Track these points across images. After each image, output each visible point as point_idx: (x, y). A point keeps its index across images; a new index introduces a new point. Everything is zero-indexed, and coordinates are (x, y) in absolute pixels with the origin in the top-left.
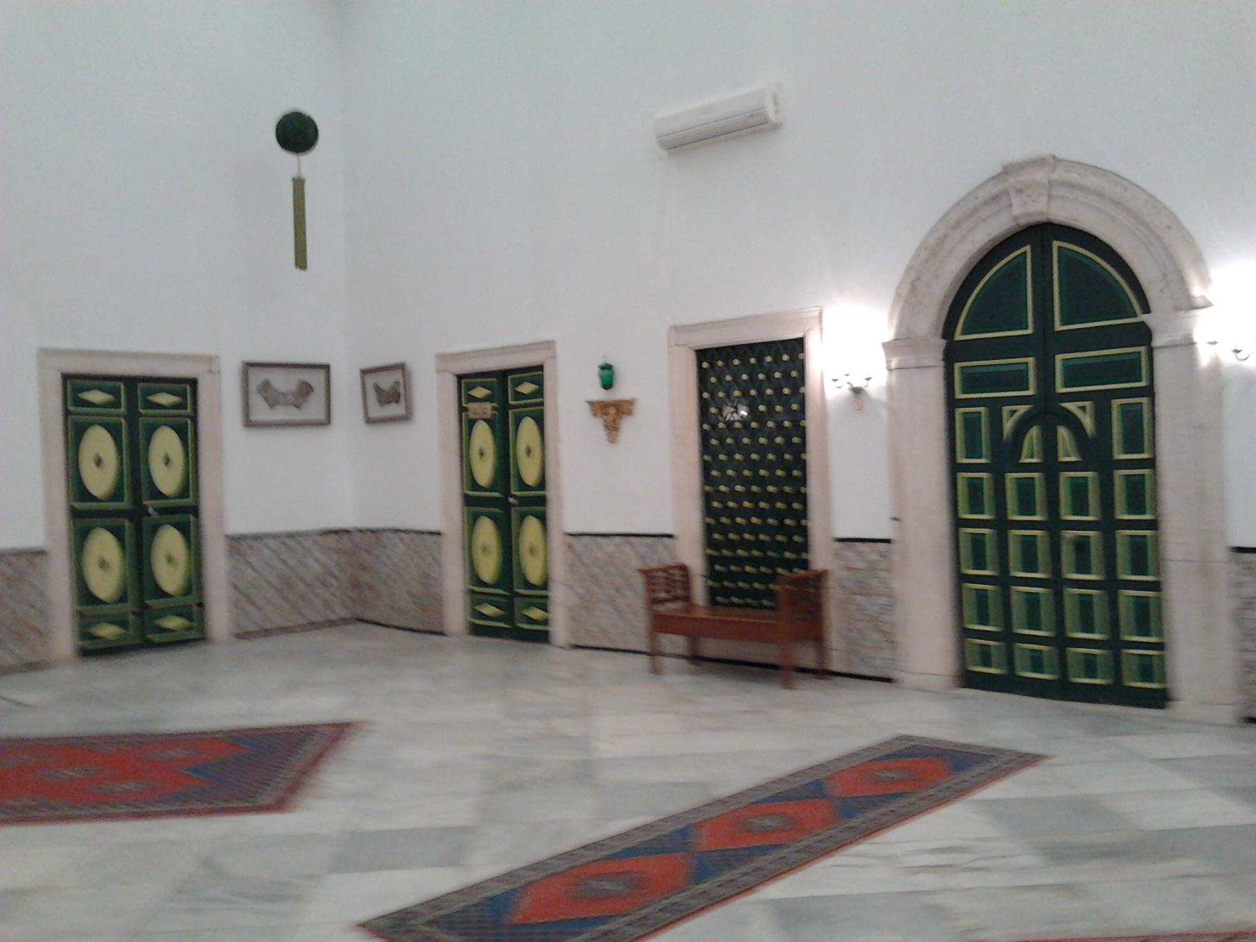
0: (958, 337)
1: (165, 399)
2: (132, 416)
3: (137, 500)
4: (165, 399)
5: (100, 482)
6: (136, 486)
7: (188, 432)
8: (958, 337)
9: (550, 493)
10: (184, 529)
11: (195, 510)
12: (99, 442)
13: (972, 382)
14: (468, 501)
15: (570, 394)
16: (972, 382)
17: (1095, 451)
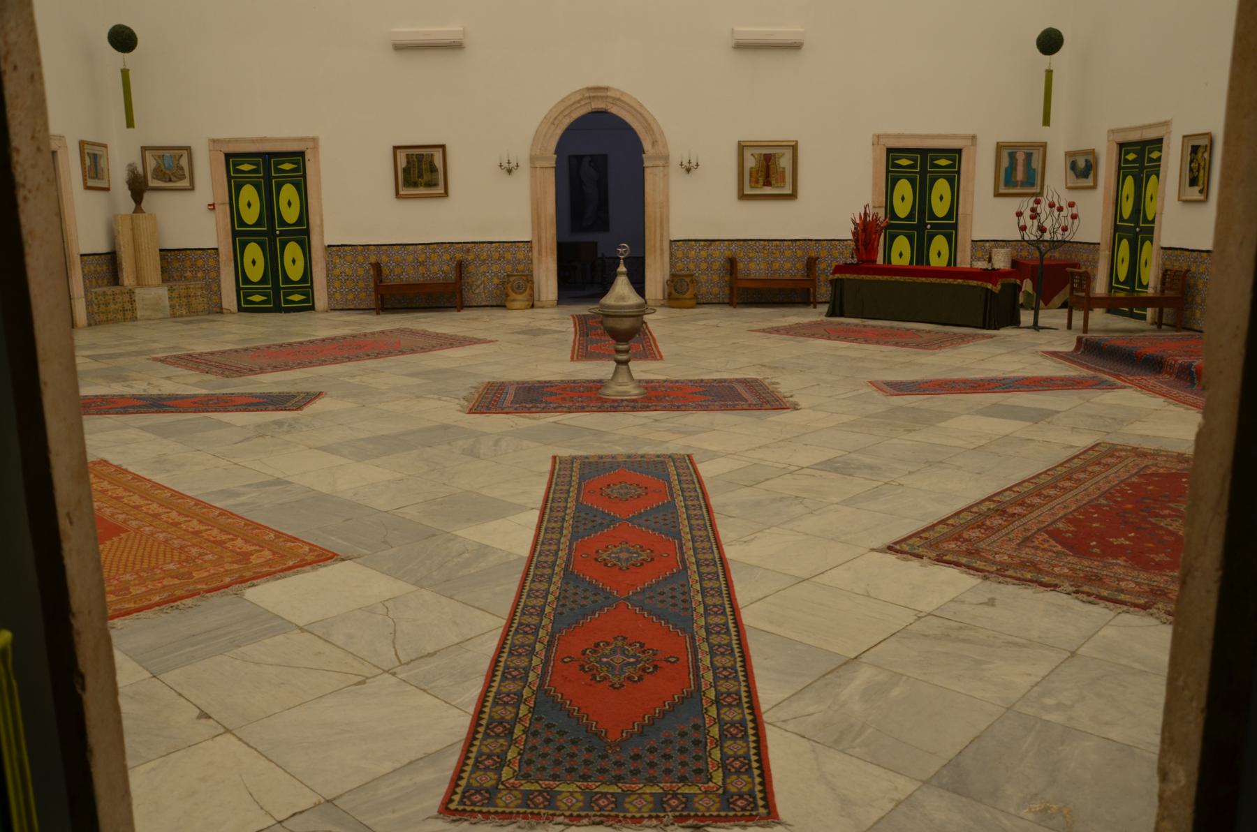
1: (943, 162)
2: (923, 173)
3: (921, 218)
4: (943, 162)
5: (902, 209)
6: (922, 212)
9: (1156, 225)
10: (949, 238)
11: (955, 227)
14: (1116, 228)
15: (1173, 161)
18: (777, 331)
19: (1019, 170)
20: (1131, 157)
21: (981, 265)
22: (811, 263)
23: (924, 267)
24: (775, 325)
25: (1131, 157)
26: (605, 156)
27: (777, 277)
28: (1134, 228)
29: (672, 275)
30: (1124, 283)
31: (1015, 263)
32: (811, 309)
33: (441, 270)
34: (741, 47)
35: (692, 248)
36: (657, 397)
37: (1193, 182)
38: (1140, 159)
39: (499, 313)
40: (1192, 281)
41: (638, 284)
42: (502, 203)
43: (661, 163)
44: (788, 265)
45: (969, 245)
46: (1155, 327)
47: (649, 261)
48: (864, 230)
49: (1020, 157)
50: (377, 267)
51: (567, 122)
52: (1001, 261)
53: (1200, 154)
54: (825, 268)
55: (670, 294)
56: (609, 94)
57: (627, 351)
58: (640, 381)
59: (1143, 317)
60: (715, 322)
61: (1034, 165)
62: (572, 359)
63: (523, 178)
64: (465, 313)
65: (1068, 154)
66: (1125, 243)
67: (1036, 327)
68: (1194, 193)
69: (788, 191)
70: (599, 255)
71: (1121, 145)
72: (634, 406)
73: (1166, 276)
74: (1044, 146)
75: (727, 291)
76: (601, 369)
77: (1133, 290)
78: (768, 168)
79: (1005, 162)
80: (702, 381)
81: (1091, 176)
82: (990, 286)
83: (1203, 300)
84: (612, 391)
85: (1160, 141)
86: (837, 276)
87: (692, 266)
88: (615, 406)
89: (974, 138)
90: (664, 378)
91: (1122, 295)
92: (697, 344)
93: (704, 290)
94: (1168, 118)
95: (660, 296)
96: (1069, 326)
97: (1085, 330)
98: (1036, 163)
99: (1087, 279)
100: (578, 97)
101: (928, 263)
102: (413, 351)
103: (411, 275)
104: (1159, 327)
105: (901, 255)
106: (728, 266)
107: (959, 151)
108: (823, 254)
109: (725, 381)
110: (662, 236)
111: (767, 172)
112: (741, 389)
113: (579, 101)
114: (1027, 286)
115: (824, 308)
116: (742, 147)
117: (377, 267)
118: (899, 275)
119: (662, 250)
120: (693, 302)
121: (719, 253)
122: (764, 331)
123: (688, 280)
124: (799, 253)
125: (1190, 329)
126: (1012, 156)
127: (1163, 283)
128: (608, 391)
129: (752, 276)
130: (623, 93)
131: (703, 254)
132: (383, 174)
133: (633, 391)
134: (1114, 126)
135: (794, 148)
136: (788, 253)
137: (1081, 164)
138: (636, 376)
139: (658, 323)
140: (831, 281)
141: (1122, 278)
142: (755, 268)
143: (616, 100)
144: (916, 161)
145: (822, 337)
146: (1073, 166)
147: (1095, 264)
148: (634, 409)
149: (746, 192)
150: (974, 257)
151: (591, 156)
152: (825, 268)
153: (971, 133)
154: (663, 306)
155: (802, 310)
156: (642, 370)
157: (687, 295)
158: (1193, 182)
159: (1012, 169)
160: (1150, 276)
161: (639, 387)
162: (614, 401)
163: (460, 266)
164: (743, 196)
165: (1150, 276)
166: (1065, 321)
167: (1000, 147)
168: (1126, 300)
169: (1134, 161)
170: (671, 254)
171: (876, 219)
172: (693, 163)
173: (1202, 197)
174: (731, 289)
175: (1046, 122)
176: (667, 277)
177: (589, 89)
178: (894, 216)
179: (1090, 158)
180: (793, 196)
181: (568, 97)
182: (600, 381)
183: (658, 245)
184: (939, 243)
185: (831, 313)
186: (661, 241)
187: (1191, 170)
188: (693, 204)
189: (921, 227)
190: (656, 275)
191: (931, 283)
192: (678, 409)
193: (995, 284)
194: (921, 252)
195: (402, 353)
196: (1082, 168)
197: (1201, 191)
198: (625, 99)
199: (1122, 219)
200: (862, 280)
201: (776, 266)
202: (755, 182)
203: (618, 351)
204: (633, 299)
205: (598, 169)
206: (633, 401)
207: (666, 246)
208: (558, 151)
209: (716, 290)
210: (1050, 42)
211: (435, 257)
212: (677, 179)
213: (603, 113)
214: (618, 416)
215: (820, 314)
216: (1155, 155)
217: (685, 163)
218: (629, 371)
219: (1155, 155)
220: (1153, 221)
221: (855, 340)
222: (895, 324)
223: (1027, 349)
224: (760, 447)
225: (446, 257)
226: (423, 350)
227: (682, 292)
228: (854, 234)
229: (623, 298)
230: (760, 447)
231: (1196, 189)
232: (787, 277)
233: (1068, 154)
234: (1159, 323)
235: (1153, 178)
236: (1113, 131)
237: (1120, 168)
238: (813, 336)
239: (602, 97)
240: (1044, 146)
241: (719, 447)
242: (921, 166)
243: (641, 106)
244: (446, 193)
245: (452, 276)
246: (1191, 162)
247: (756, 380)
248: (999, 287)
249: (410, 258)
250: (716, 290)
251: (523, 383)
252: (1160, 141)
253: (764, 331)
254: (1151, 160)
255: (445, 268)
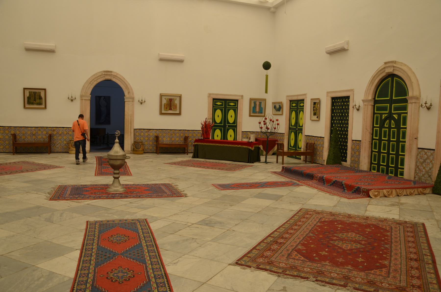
0: (376, 99)
1: (232, 104)
2: (225, 107)
4: (232, 104)
5: (218, 120)
7: (236, 111)
8: (376, 99)
9: (303, 128)
11: (236, 126)
12: (218, 112)
13: (379, 109)
14: (290, 128)
15: (308, 107)
16: (379, 109)
17: (397, 122)
18: (175, 163)
19: (257, 108)
20: (294, 105)
21: (245, 140)
22: (186, 138)
23: (226, 141)
24: (174, 161)
25: (294, 105)
26: (109, 98)
27: (173, 143)
28: (296, 129)
29: (135, 142)
30: (293, 147)
31: (256, 140)
32: (186, 155)
33: (42, 137)
34: (162, 60)
35: (142, 132)
36: (132, 192)
37: (315, 114)
38: (297, 106)
39: (66, 155)
40: (316, 147)
41: (122, 145)
42: (67, 112)
43: (131, 100)
44: (177, 139)
45: (241, 132)
46: (304, 162)
47: (126, 136)
48: (205, 127)
49: (258, 103)
50: (14, 136)
51: (95, 83)
52: (252, 140)
53: (316, 105)
54: (191, 140)
55: (134, 149)
56: (112, 74)
57: (118, 174)
58: (123, 185)
59: (300, 159)
60: (151, 160)
61: (262, 107)
62: (95, 175)
63: (78, 103)
64: (52, 155)
65: (273, 103)
66: (293, 133)
67: (266, 162)
68: (315, 118)
69: (178, 112)
70: (106, 133)
71: (291, 101)
72: (121, 196)
73: (308, 145)
74: (265, 100)
75: (155, 148)
76: (107, 180)
77: (296, 150)
78: (171, 103)
79: (253, 105)
80: (148, 184)
81: (281, 111)
82: (250, 148)
83: (320, 153)
84: (112, 190)
85: (303, 100)
86: (196, 143)
87: (142, 139)
88: (114, 196)
89: (242, 96)
90: (132, 183)
91: (292, 151)
92: (146, 169)
93: (146, 147)
94: (305, 93)
95: (130, 149)
96: (277, 162)
97: (283, 164)
98: (263, 106)
99: (282, 145)
100: (100, 74)
101: (227, 139)
102: (27, 171)
103: (29, 139)
104: (306, 162)
105: (218, 136)
106: (155, 139)
107: (237, 101)
108: (190, 135)
109: (157, 184)
110: (131, 127)
111: (170, 105)
112: (163, 188)
113: (100, 76)
114: (261, 147)
115: (191, 155)
116: (161, 96)
117: (14, 136)
118: (219, 143)
119: (131, 132)
120: (142, 152)
121: (152, 134)
122: (170, 164)
123: (141, 144)
124: (182, 135)
125: (316, 163)
126: (255, 103)
127: (307, 147)
128: (110, 190)
129: (164, 143)
130: (117, 74)
131: (146, 134)
132: (19, 99)
133: (120, 189)
134: (288, 95)
135: (180, 97)
136: (177, 135)
137: (278, 106)
138: (122, 182)
139: (132, 162)
140: (194, 145)
141: (292, 145)
142: (165, 140)
143: (115, 76)
144: (223, 103)
145: (191, 166)
146: (275, 107)
147: (283, 140)
148: (122, 197)
149: (163, 112)
150: (243, 137)
151: (104, 97)
152: (191, 140)
153: (241, 94)
154: (131, 153)
155: (183, 155)
156: (124, 180)
157: (140, 150)
158: (315, 114)
159: (255, 107)
160: (302, 144)
161: (123, 188)
162: (113, 194)
163: (50, 136)
164: (161, 114)
165: (302, 144)
166: (276, 160)
167: (251, 100)
168: (294, 153)
169: (295, 106)
170: (134, 134)
171: (209, 124)
172: (143, 101)
173: (318, 119)
174: (157, 147)
175: (266, 92)
176: (133, 142)
177: (104, 71)
178: (216, 123)
179: (281, 105)
180: (179, 114)
181: (96, 74)
182: (107, 185)
183: (129, 130)
184: (231, 132)
185: (194, 157)
186: (131, 129)
187: (314, 110)
188: (143, 116)
189: (224, 126)
190: (129, 141)
191: (230, 147)
192: (139, 197)
193: (252, 147)
194: (224, 135)
195: (22, 172)
196: (278, 108)
197: (317, 117)
198: (118, 76)
199: (292, 126)
200: (205, 145)
201: (173, 139)
202: (166, 109)
203: (115, 174)
204: (121, 153)
205: (106, 103)
206: (121, 194)
207: (132, 131)
208: (91, 94)
209: (151, 148)
210: (267, 66)
211: (40, 132)
212: (137, 106)
213: (110, 81)
214: (115, 201)
215: (190, 157)
216: (302, 105)
217: (140, 101)
218: (119, 182)
219: (302, 105)
220: (302, 126)
221: (204, 167)
222: (217, 161)
223: (263, 171)
224: (175, 215)
225: (44, 133)
226: (32, 171)
227: (138, 148)
228: (202, 128)
229: (117, 152)
230: (175, 215)
231: (316, 116)
232: (177, 143)
233: (273, 103)
234: (306, 161)
235: (301, 112)
236: (288, 96)
237: (290, 108)
238: (188, 166)
239: (109, 75)
240: (265, 100)
241: (156, 213)
242: (224, 105)
243: (124, 79)
244: (45, 107)
245: (47, 140)
246: (314, 107)
247: (169, 184)
248: (253, 148)
249: (29, 132)
250: (151, 148)
251: (74, 186)
252: (303, 100)
253: (170, 164)
254: (300, 106)
255: (44, 137)
